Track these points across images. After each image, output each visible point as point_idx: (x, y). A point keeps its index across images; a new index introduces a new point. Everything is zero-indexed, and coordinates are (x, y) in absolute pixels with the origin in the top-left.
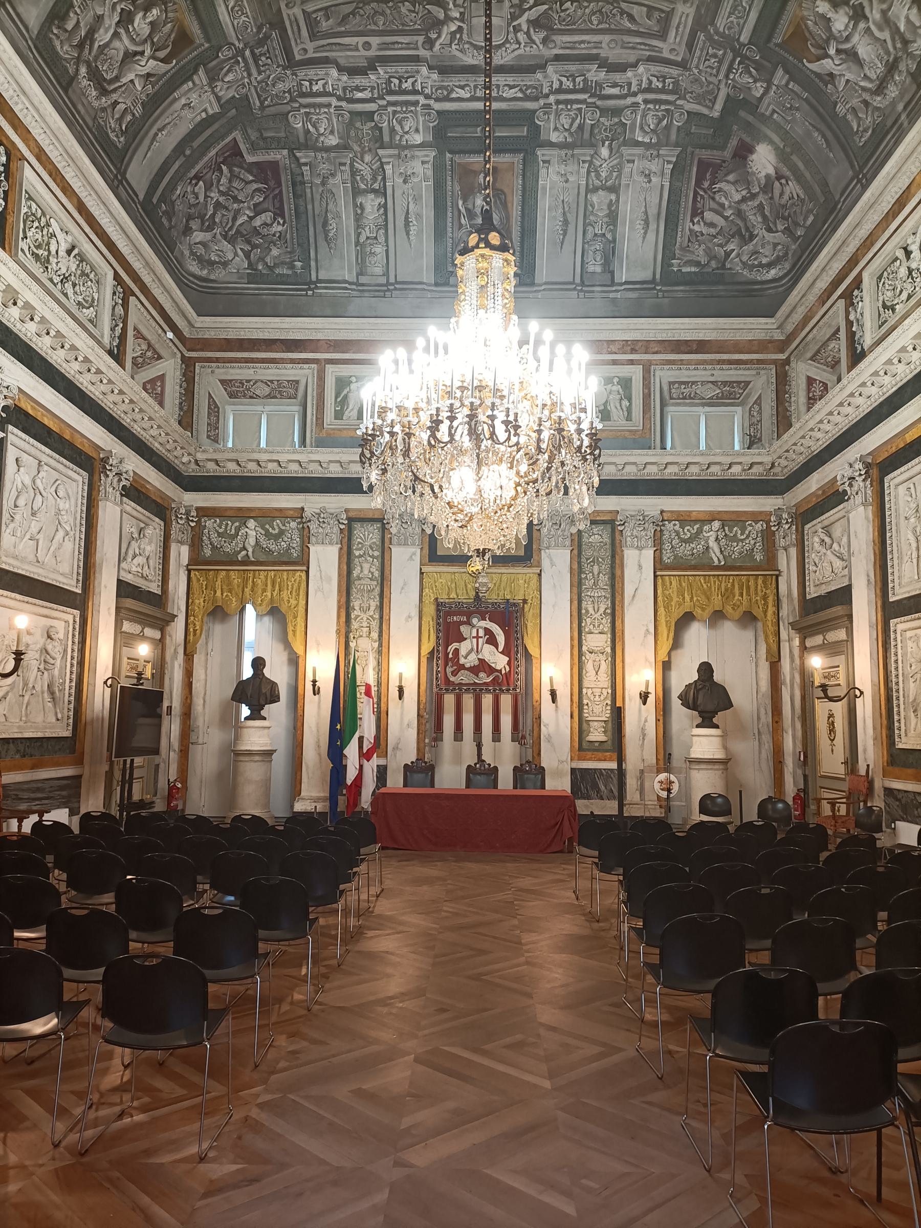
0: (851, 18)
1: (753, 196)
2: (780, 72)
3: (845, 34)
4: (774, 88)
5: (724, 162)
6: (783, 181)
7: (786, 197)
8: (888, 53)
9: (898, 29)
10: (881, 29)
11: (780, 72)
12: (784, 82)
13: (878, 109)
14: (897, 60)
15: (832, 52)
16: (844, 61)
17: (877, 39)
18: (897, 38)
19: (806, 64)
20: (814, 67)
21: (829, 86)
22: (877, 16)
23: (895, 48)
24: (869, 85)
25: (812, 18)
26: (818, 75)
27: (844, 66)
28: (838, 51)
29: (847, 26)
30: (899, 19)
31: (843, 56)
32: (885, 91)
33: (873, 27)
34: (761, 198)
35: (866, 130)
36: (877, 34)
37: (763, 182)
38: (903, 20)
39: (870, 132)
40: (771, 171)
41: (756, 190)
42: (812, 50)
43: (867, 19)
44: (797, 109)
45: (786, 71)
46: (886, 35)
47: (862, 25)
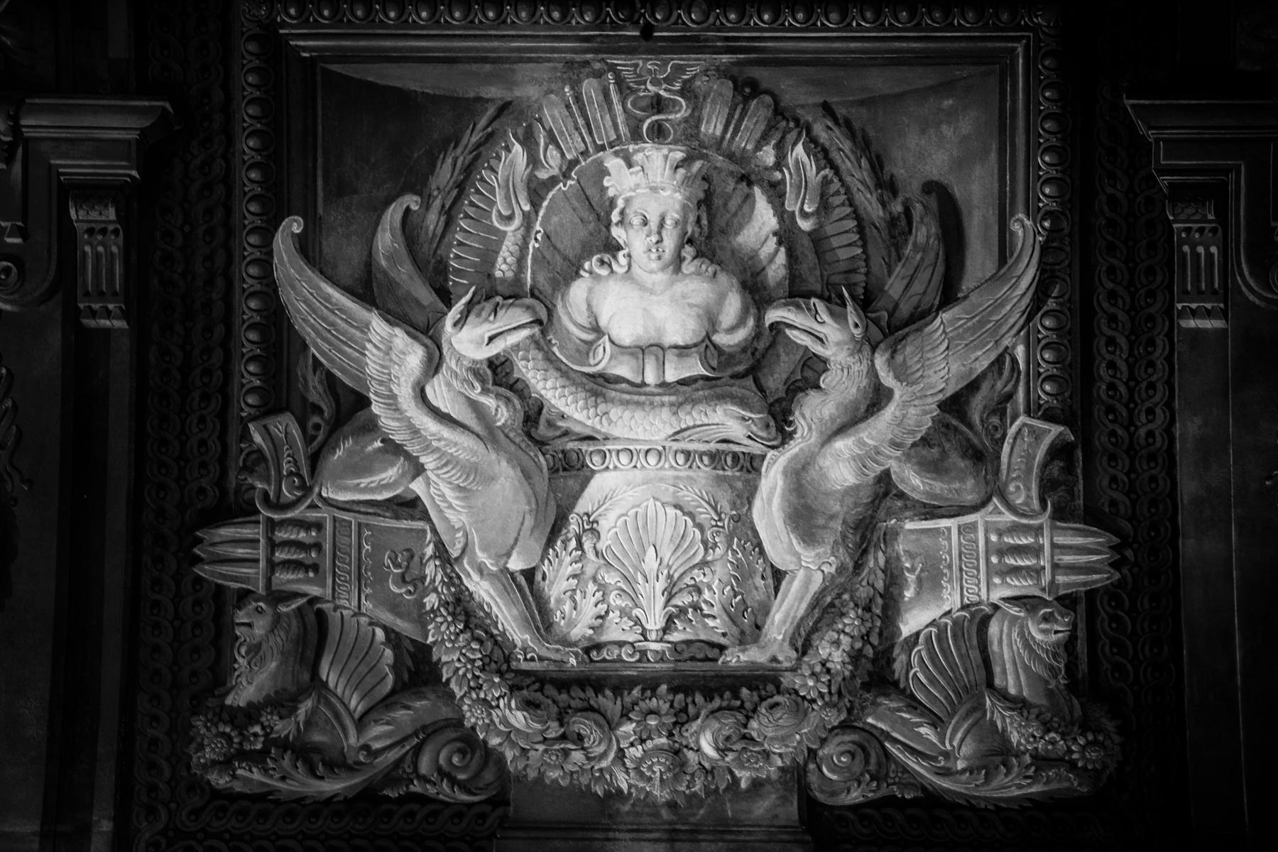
0: (706, 346)
2: (119, 124)
3: (602, 360)
8: (750, 626)
9: (887, 605)
10: (804, 518)
11: (119, 124)
13: (469, 742)
14: (764, 683)
16: (489, 434)
17: (742, 530)
18: (851, 621)
19: (283, 245)
21: (285, 425)
22: (841, 469)
23: (803, 643)
24: (508, 618)
25: (552, 162)
27: (463, 445)
28: (498, 373)
30: (931, 581)
31: (503, 414)
32: (582, 725)
33: (773, 479)
35: (307, 755)
36: (769, 511)
38: (951, 600)
39: (332, 786)
42: (386, 239)
43: (780, 421)
46: (808, 568)
47: (729, 422)
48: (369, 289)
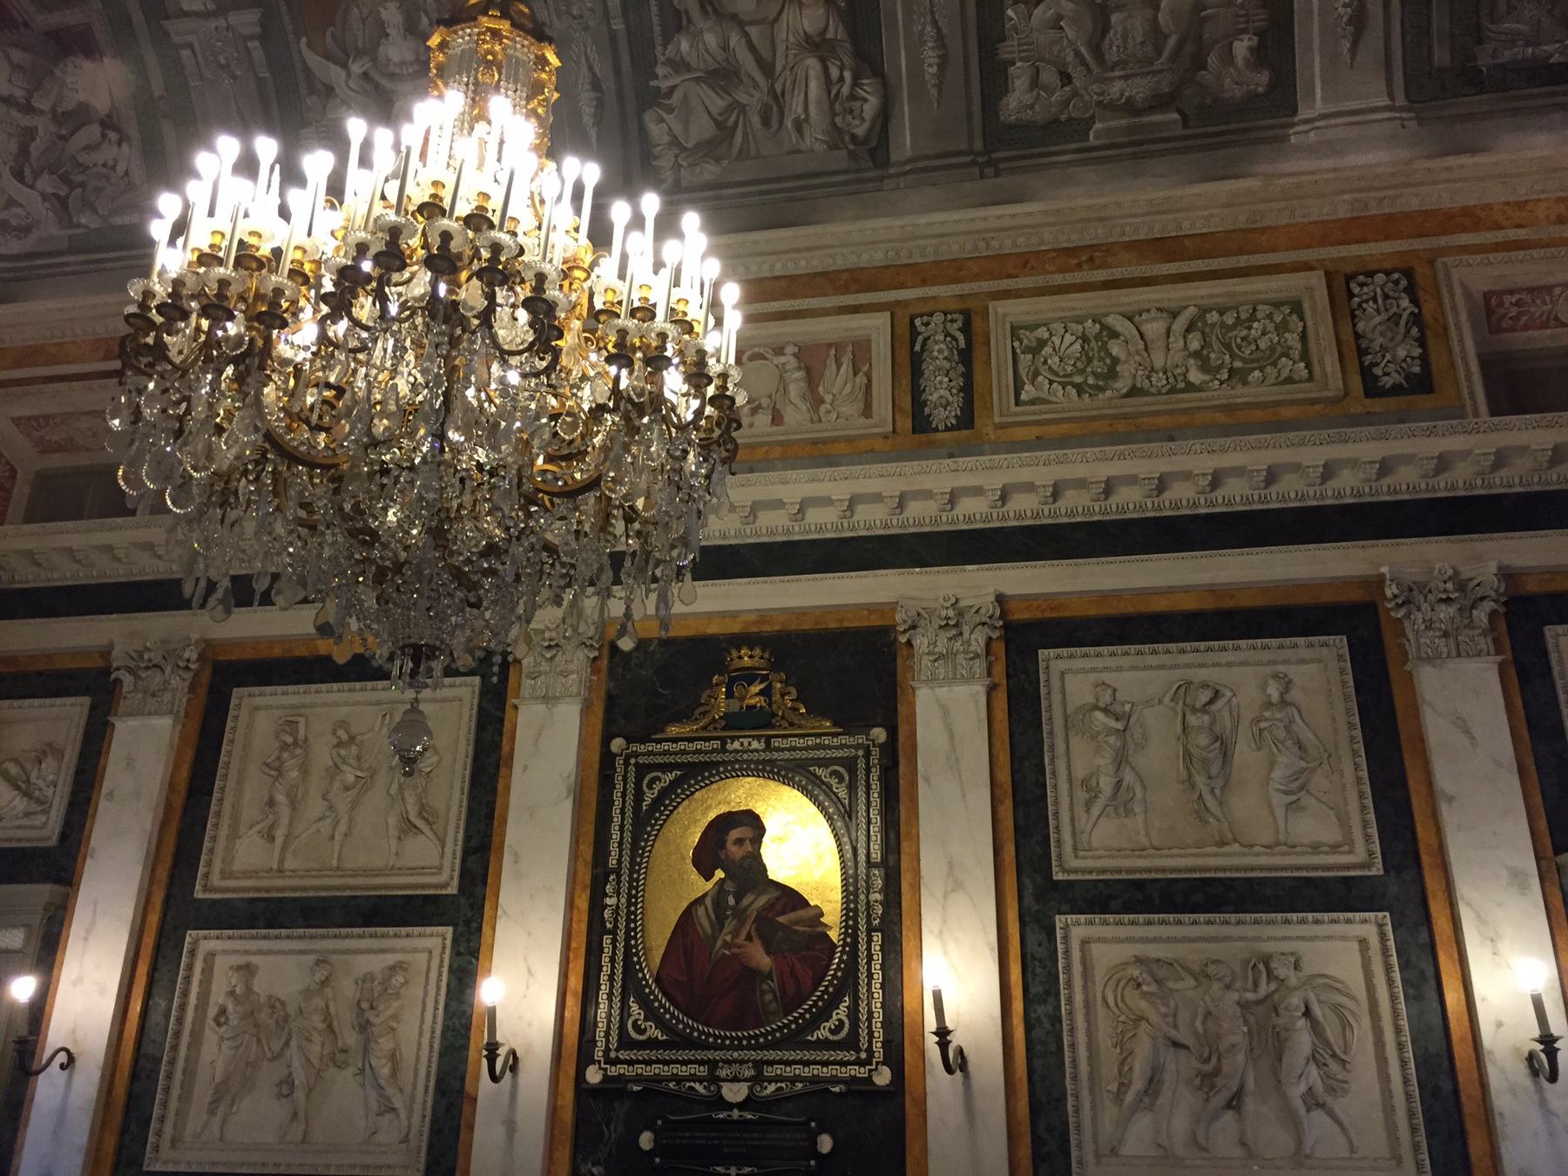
1: (28, 109)
3: (391, 68)
4: (222, 23)
5: (26, 25)
6: (113, 136)
7: (99, 157)
12: (246, 31)
15: (356, 68)
20: (313, 60)
25: (366, 11)
26: (307, 71)
29: (403, 64)
31: (369, 87)
34: (42, 124)
37: (67, 106)
40: (101, 104)
41: (43, 104)
44: (234, 77)
45: (262, 24)
48: (328, 56)
